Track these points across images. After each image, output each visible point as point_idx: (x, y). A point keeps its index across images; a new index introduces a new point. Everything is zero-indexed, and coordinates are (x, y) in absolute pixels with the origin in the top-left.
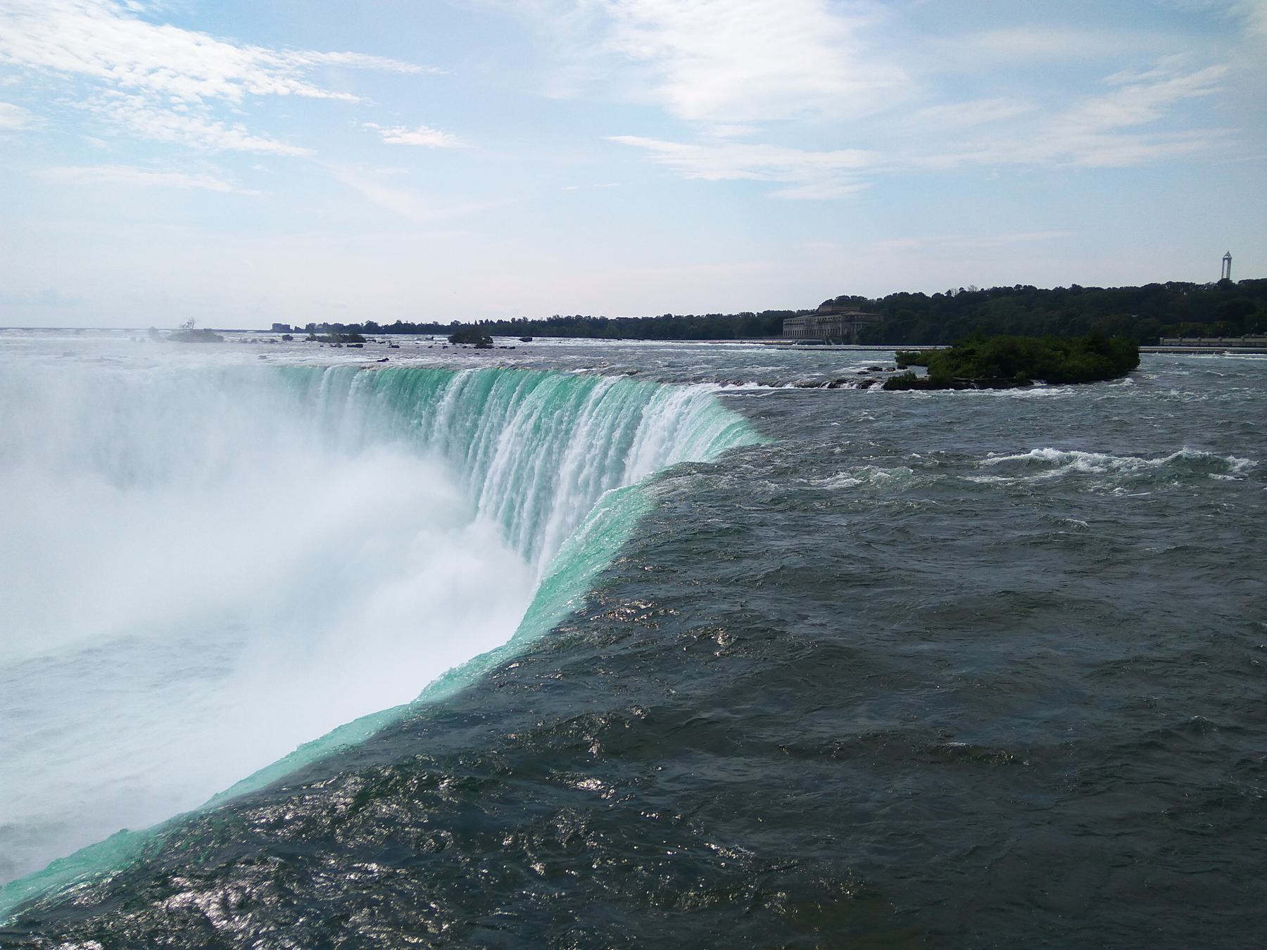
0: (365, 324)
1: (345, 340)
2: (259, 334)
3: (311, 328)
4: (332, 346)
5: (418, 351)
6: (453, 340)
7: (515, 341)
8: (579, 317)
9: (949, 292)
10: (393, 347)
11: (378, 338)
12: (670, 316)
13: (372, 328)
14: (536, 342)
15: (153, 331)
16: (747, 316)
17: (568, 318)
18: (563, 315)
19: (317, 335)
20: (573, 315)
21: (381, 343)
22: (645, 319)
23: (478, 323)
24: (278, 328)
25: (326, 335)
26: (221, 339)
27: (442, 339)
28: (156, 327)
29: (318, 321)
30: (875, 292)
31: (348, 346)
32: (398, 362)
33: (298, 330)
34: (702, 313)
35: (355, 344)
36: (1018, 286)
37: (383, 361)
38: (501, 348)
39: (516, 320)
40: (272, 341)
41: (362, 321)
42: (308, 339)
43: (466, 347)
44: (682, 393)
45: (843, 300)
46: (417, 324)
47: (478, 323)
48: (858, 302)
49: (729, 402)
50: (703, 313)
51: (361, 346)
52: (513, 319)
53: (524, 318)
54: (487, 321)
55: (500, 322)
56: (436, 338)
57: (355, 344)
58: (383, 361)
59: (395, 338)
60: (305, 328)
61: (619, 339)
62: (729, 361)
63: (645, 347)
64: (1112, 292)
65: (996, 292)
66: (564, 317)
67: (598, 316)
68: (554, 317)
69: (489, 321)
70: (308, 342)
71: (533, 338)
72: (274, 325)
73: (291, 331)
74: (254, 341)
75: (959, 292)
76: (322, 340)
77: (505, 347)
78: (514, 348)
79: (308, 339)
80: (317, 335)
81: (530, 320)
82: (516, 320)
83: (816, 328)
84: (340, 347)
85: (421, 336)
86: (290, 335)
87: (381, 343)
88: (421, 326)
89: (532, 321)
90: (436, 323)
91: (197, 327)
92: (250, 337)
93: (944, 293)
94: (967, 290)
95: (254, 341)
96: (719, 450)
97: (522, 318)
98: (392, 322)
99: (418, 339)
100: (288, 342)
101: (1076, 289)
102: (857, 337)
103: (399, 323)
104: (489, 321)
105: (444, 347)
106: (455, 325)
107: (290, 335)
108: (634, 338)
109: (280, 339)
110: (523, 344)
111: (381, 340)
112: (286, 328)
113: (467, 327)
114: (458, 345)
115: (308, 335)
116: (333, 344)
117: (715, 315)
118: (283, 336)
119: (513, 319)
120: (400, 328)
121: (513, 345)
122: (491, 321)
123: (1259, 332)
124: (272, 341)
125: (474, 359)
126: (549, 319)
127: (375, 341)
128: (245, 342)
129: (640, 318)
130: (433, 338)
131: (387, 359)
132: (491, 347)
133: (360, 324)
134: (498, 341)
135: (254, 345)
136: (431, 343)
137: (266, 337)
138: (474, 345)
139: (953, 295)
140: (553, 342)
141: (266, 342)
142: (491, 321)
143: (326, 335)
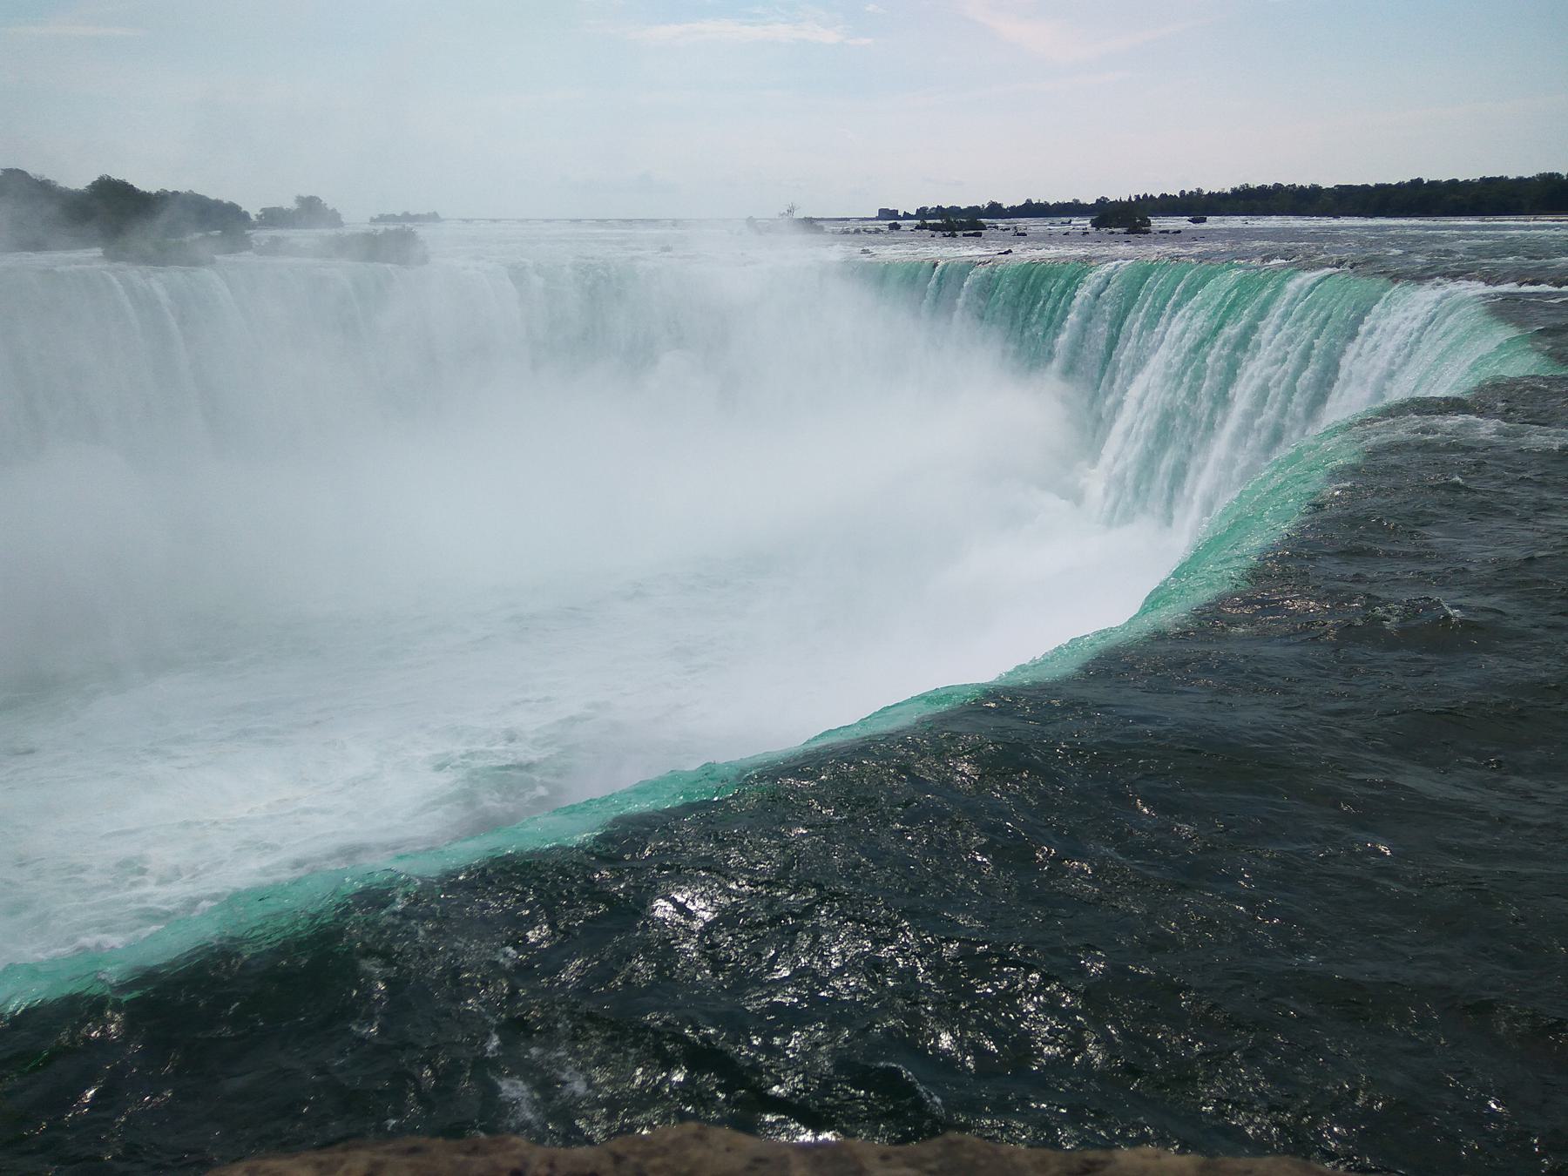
0: (987, 206)
1: (962, 227)
2: (866, 223)
3: (922, 213)
4: (945, 236)
5: (1049, 238)
6: (1094, 224)
7: (1182, 223)
8: (1278, 187)
10: (1018, 235)
11: (1001, 223)
12: (1420, 181)
13: (995, 210)
14: (1213, 222)
15: (751, 221)
17: (1263, 189)
18: (1255, 183)
19: (928, 221)
20: (1270, 183)
21: (1004, 230)
22: (1379, 187)
23: (1133, 199)
24: (886, 214)
25: (939, 221)
27: (1086, 222)
28: (755, 217)
29: (931, 205)
31: (964, 235)
32: (1024, 253)
33: (907, 216)
34: (1473, 174)
35: (972, 232)
37: (1006, 253)
38: (1161, 232)
39: (1187, 193)
40: (877, 231)
41: (983, 202)
42: (918, 227)
43: (1113, 233)
44: (1425, 297)
46: (1051, 204)
47: (1133, 199)
49: (1504, 310)
51: (980, 235)
52: (1182, 192)
53: (1198, 190)
54: (1145, 196)
55: (1164, 196)
56: (1075, 221)
57: (972, 232)
58: (1006, 253)
59: (1022, 223)
60: (915, 213)
61: (1336, 216)
62: (1512, 248)
63: (1376, 228)
66: (1255, 187)
67: (1307, 184)
68: (1242, 187)
69: (1149, 196)
70: (917, 231)
71: (1208, 218)
73: (900, 218)
74: (857, 231)
76: (934, 228)
77: (1167, 232)
78: (1179, 232)
79: (918, 227)
80: (928, 221)
81: (1206, 193)
82: (1187, 193)
84: (955, 236)
85: (1057, 220)
86: (898, 222)
87: (1004, 230)
88: (1058, 205)
89: (1210, 193)
92: (851, 226)
95: (857, 231)
96: (1471, 382)
97: (1195, 191)
98: (1020, 202)
99: (1051, 224)
100: (895, 232)
104: (1149, 196)
105: (1084, 234)
106: (1102, 202)
107: (898, 222)
108: (1358, 215)
109: (886, 229)
110: (1193, 226)
111: (1004, 226)
112: (892, 214)
113: (1119, 205)
114: (1103, 230)
115: (918, 222)
116: (947, 234)
117: (1495, 178)
118: (890, 225)
119: (1182, 192)
120: (1032, 210)
121: (1177, 229)
122: (1151, 196)
124: (877, 231)
125: (1123, 248)
126: (1234, 190)
127: (996, 227)
128: (847, 232)
129: (1372, 184)
130: (1070, 222)
131: (1010, 251)
132: (1147, 232)
133: (980, 205)
134: (1157, 223)
135: (857, 236)
136: (1067, 228)
137: (871, 226)
138: (1124, 230)
140: (1236, 222)
141: (870, 232)
142: (1151, 196)
143: (939, 221)
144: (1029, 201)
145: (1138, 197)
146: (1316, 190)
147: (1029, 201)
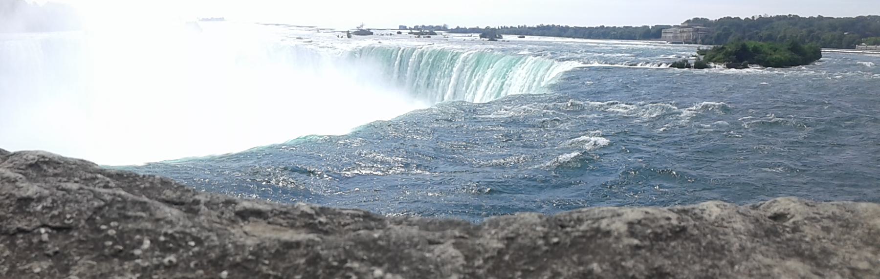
8: (553, 26)
9: (753, 17)
13: (444, 28)
16: (645, 27)
18: (545, 24)
20: (551, 24)
26: (372, 34)
30: (713, 17)
36: (790, 15)
39: (520, 26)
45: (696, 20)
48: (704, 22)
50: (622, 26)
55: (511, 27)
61: (574, 38)
64: (839, 20)
65: (779, 18)
72: (400, 26)
75: (758, 17)
82: (520, 26)
83: (679, 35)
90: (478, 27)
91: (364, 28)
93: (750, 17)
94: (763, 16)
98: (454, 27)
101: (820, 18)
102: (700, 40)
103: (458, 28)
109: (396, 33)
119: (519, 26)
120: (458, 30)
123: (876, 43)
139: (755, 19)
144: (458, 27)
145: (502, 27)
146: (567, 28)
147: (458, 27)
